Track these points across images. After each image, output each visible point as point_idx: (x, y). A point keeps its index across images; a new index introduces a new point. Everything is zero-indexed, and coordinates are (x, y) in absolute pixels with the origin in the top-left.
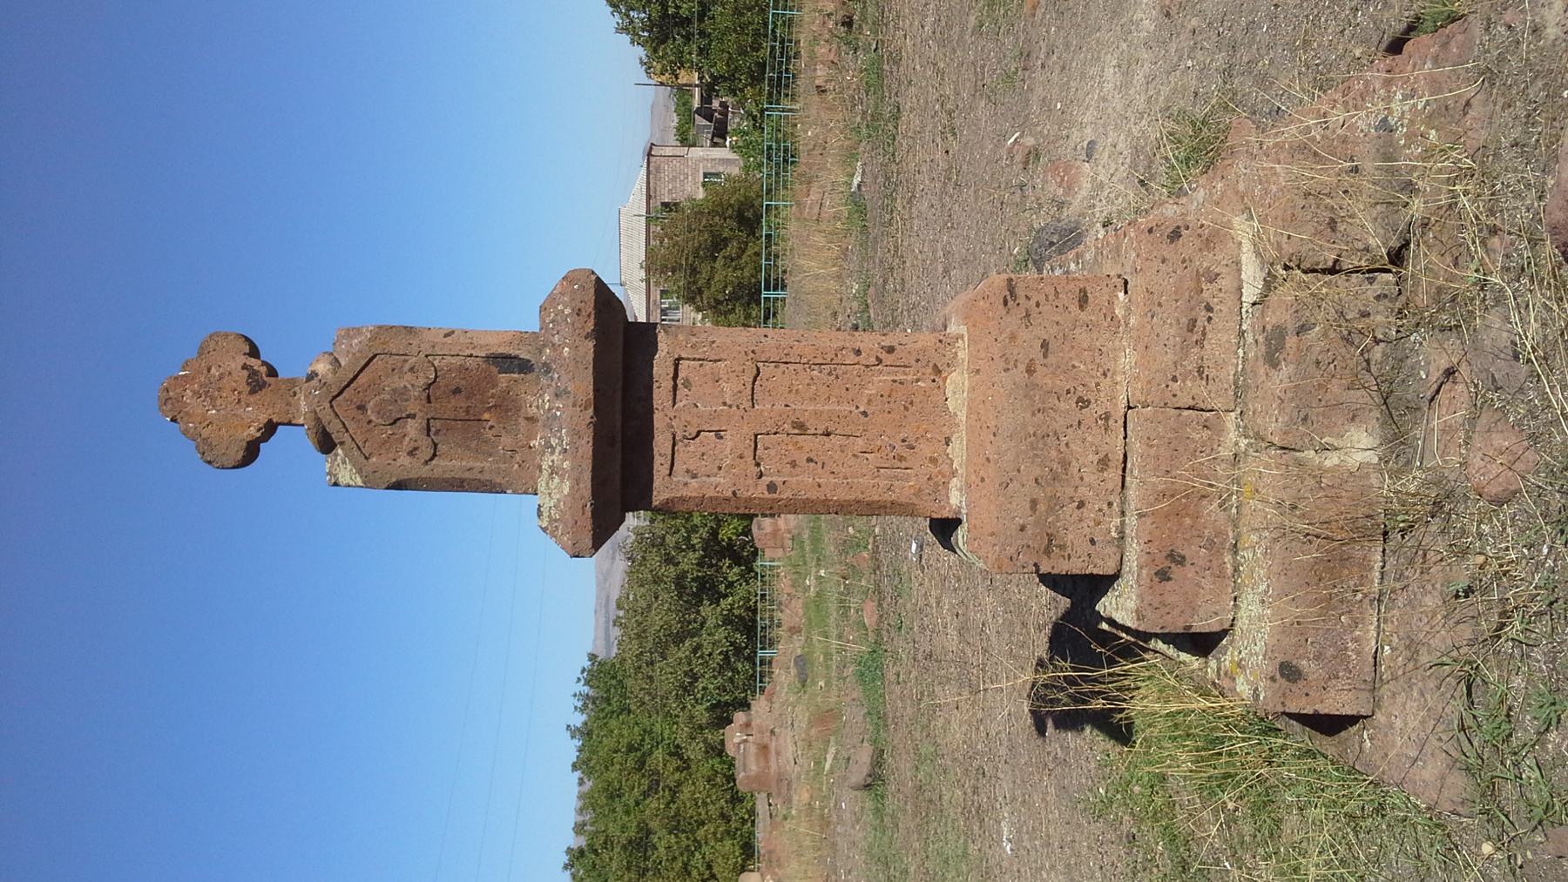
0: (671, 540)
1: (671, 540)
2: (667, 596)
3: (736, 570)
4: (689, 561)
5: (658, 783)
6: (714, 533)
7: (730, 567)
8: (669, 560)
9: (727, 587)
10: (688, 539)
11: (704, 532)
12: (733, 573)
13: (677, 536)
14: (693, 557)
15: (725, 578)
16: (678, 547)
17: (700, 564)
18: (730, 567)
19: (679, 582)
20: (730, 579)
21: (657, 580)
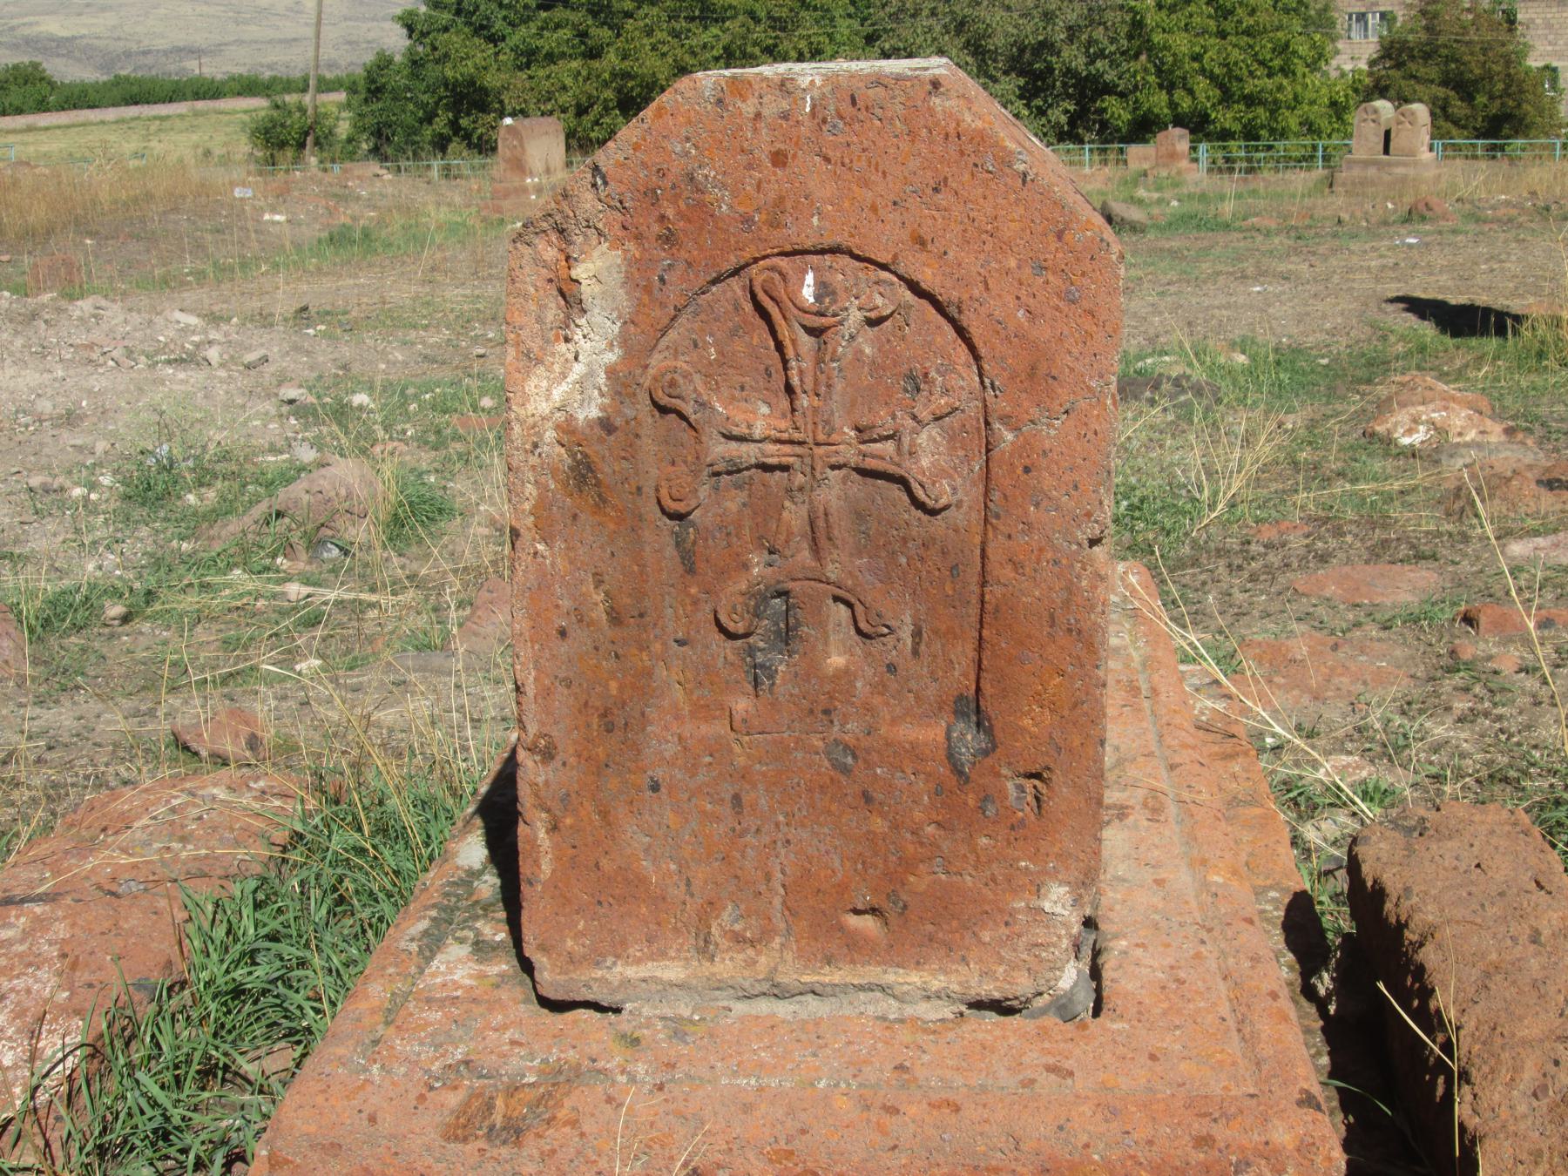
0: (1099, 33)
1: (1099, 33)
2: (1031, 32)
3: (1063, 119)
4: (1074, 57)
5: (783, 29)
6: (1109, 89)
7: (1066, 111)
8: (1072, 32)
9: (1039, 108)
10: (1101, 54)
11: (1111, 76)
12: (1058, 115)
13: (1106, 42)
14: (1079, 63)
15: (1050, 106)
16: (1091, 42)
17: (1069, 72)
18: (1066, 111)
19: (1045, 46)
20: (1050, 112)
21: (1048, 17)
